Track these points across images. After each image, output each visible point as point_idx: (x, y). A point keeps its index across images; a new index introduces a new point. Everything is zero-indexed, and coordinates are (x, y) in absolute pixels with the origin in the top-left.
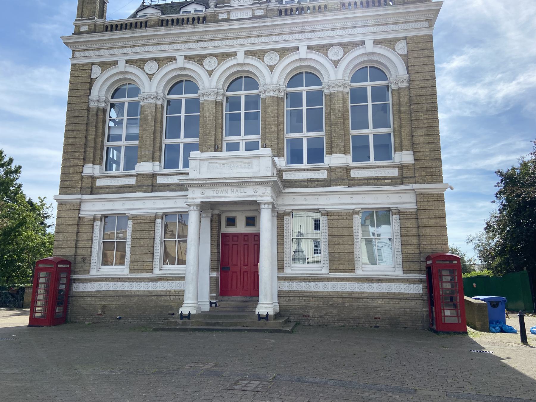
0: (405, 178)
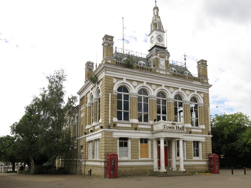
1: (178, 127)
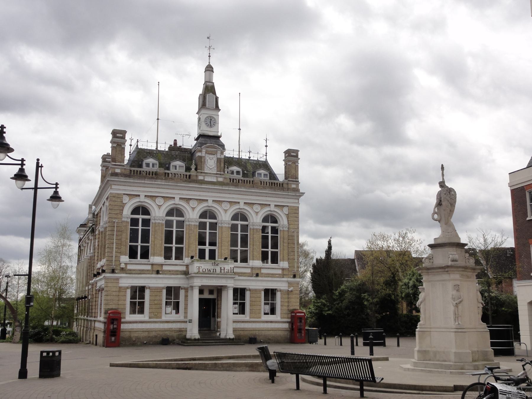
1: (222, 268)
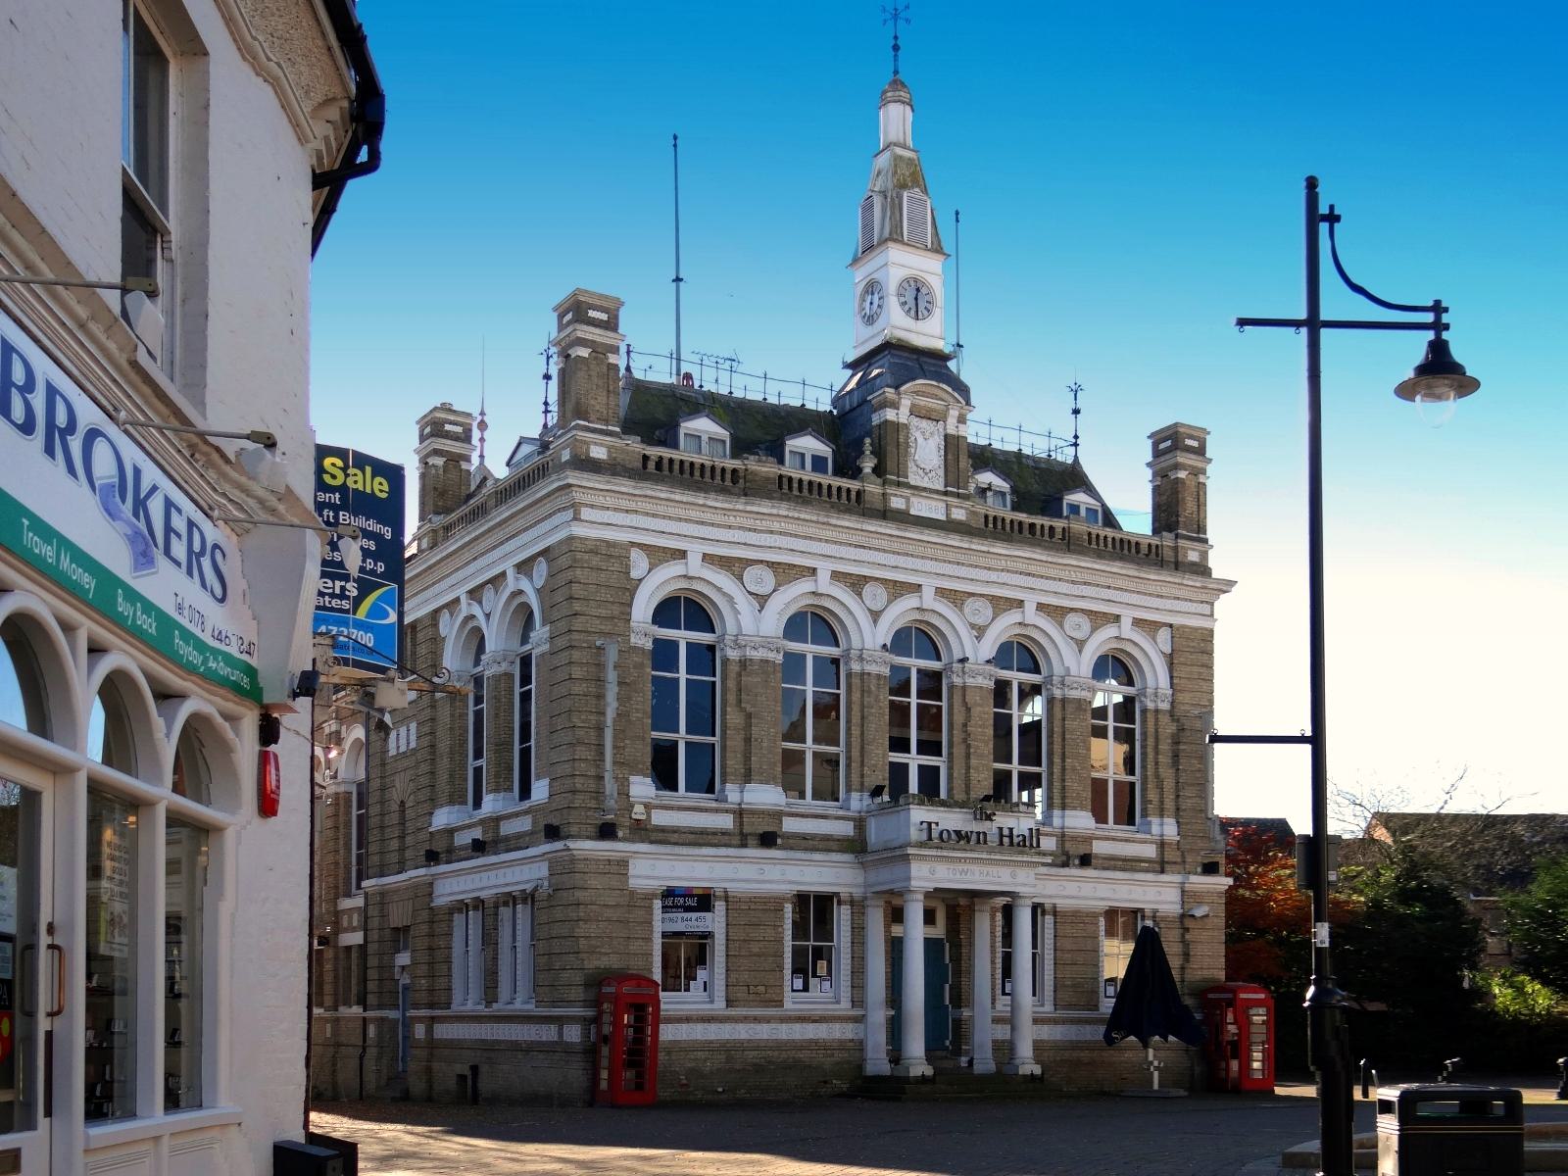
0: (1167, 863)
1: (1006, 832)
